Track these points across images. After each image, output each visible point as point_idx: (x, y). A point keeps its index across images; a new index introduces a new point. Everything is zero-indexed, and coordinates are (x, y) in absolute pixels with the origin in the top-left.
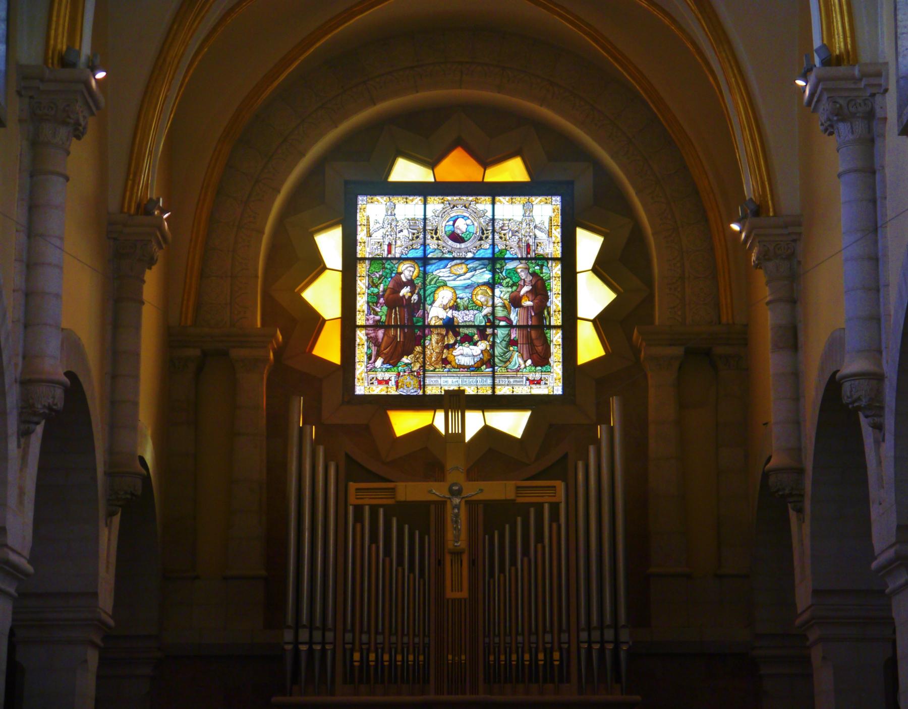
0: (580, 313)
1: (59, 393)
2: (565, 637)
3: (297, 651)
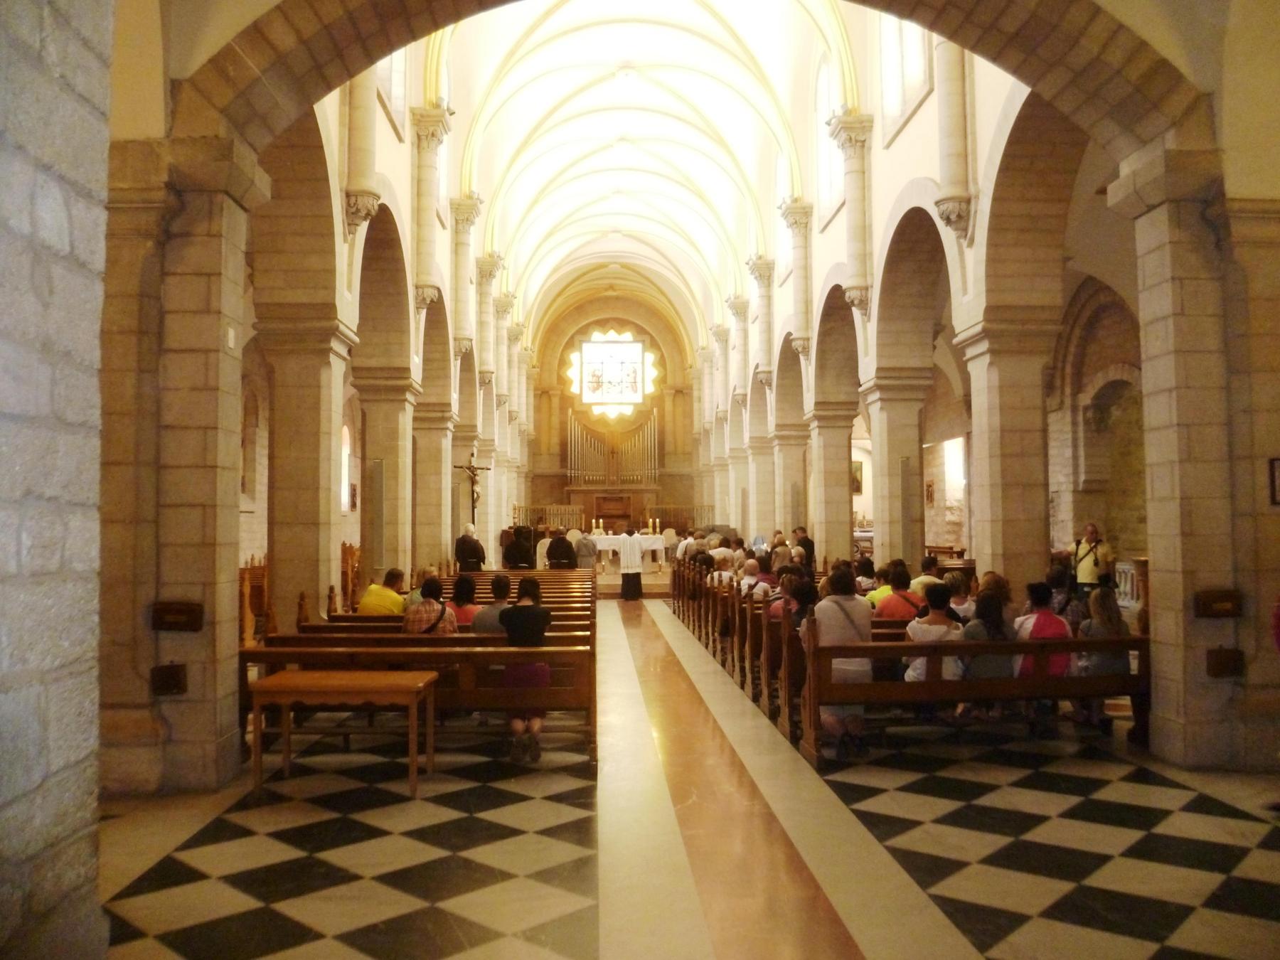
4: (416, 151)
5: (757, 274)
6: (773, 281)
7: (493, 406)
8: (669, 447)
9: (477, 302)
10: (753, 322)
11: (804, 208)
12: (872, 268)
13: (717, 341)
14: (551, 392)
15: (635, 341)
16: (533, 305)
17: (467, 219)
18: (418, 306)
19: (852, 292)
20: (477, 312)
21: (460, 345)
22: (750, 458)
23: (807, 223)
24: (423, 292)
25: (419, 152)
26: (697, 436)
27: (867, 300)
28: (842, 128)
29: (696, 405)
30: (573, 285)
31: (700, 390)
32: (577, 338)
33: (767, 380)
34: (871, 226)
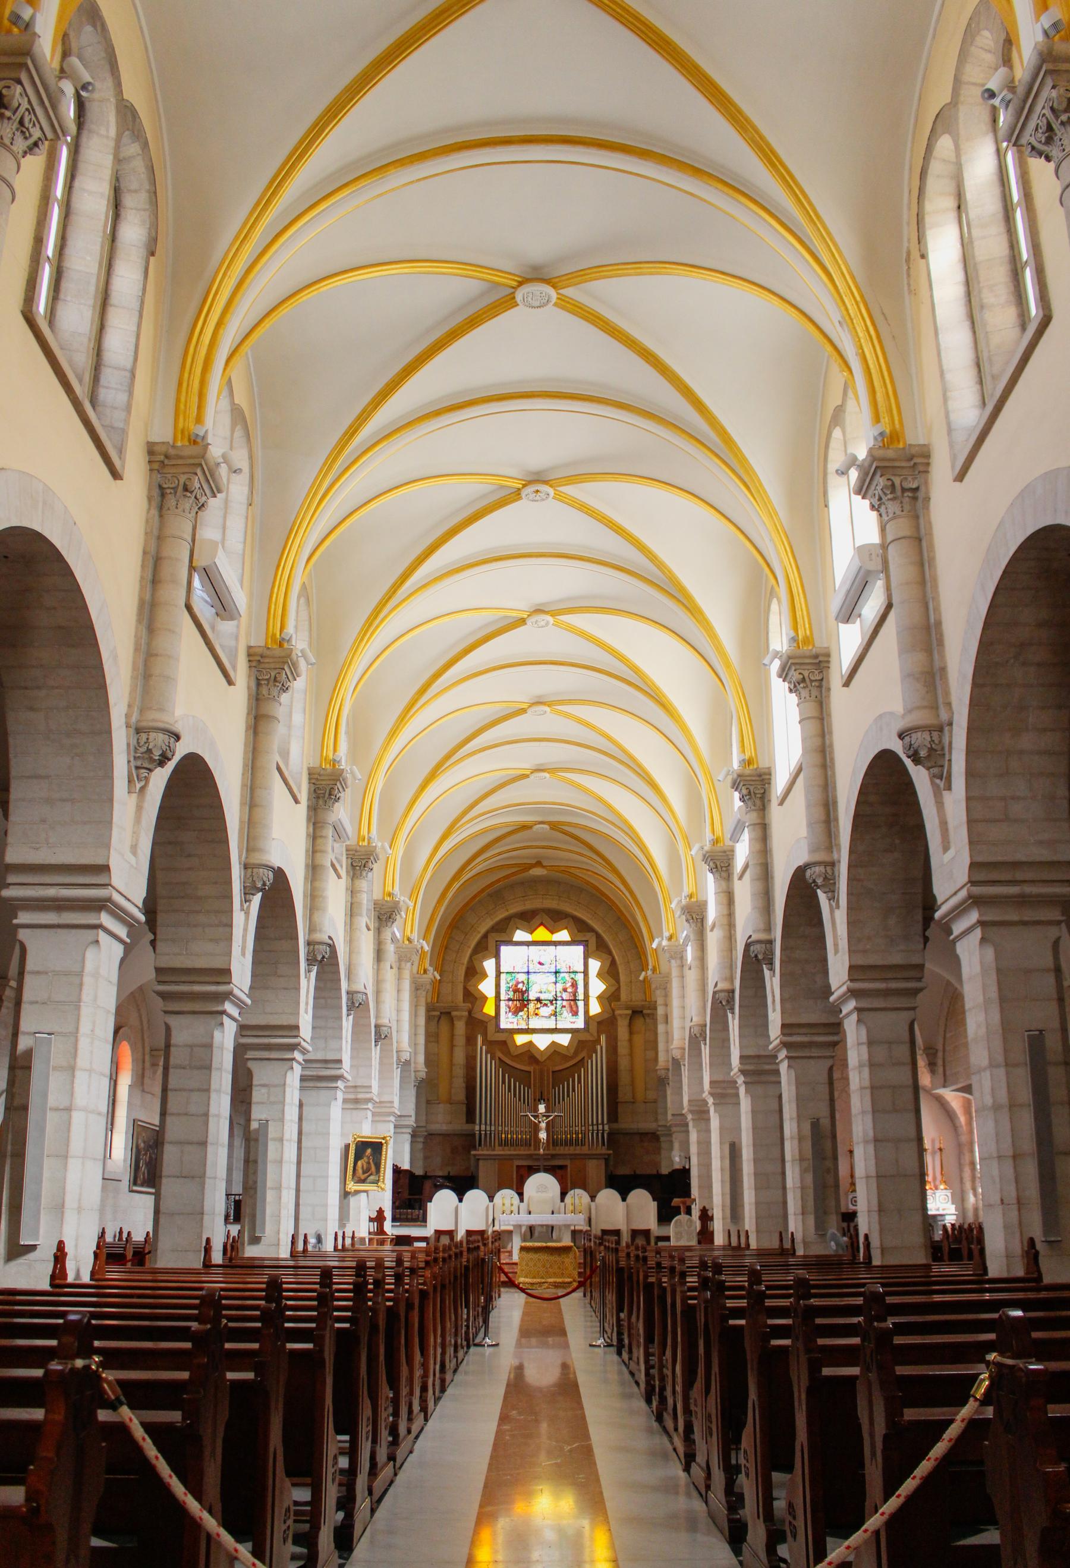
0: (591, 994)
1: (408, 1054)
2: (583, 1128)
3: (480, 1134)
4: (155, 512)
5: (744, 792)
6: (770, 801)
7: (341, 1008)
8: (624, 1094)
9: (308, 835)
10: (740, 878)
11: (816, 656)
12: (947, 693)
13: (687, 920)
14: (454, 1013)
15: (573, 942)
16: (422, 876)
17: (275, 680)
18: (139, 763)
19: (914, 735)
20: (307, 851)
21: (252, 876)
22: (742, 1090)
23: (822, 680)
24: (148, 739)
25: (161, 516)
26: (663, 1072)
27: (943, 749)
28: (877, 468)
29: (661, 1028)
30: (482, 857)
31: (666, 1005)
32: (493, 938)
33: (765, 953)
34: (939, 624)
